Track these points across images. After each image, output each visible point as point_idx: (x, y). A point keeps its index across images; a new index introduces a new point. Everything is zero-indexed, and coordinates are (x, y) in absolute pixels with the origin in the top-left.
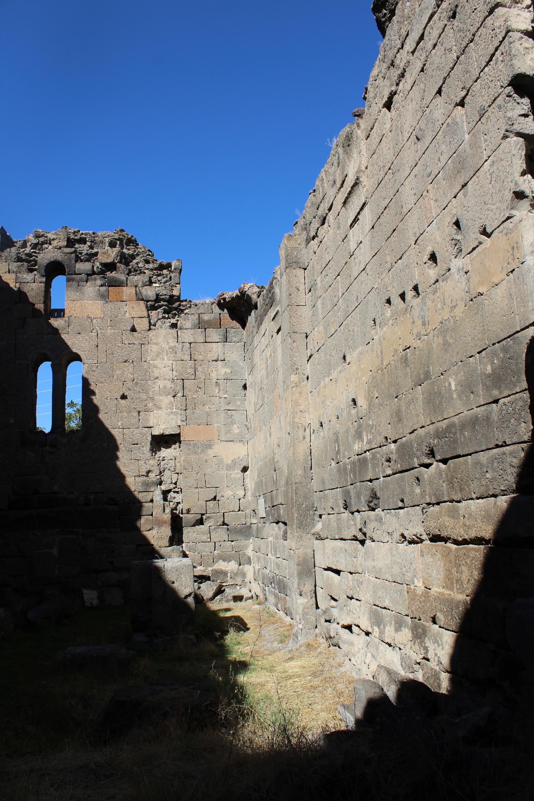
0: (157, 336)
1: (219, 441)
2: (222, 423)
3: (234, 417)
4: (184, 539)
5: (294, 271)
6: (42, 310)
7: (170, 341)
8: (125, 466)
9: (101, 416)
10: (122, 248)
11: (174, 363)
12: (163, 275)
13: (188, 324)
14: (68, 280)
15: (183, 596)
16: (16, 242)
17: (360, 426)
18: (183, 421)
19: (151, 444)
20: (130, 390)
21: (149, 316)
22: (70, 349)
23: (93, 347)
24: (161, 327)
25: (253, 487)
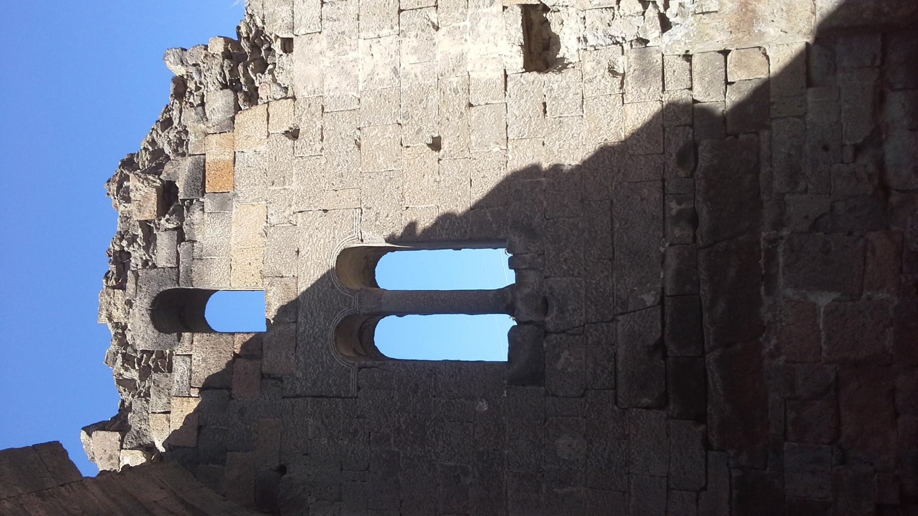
7: (317, 48)
8: (598, 128)
11: (362, 35)
13: (284, 12)
16: (123, 402)
22: (328, 272)
23: (326, 219)
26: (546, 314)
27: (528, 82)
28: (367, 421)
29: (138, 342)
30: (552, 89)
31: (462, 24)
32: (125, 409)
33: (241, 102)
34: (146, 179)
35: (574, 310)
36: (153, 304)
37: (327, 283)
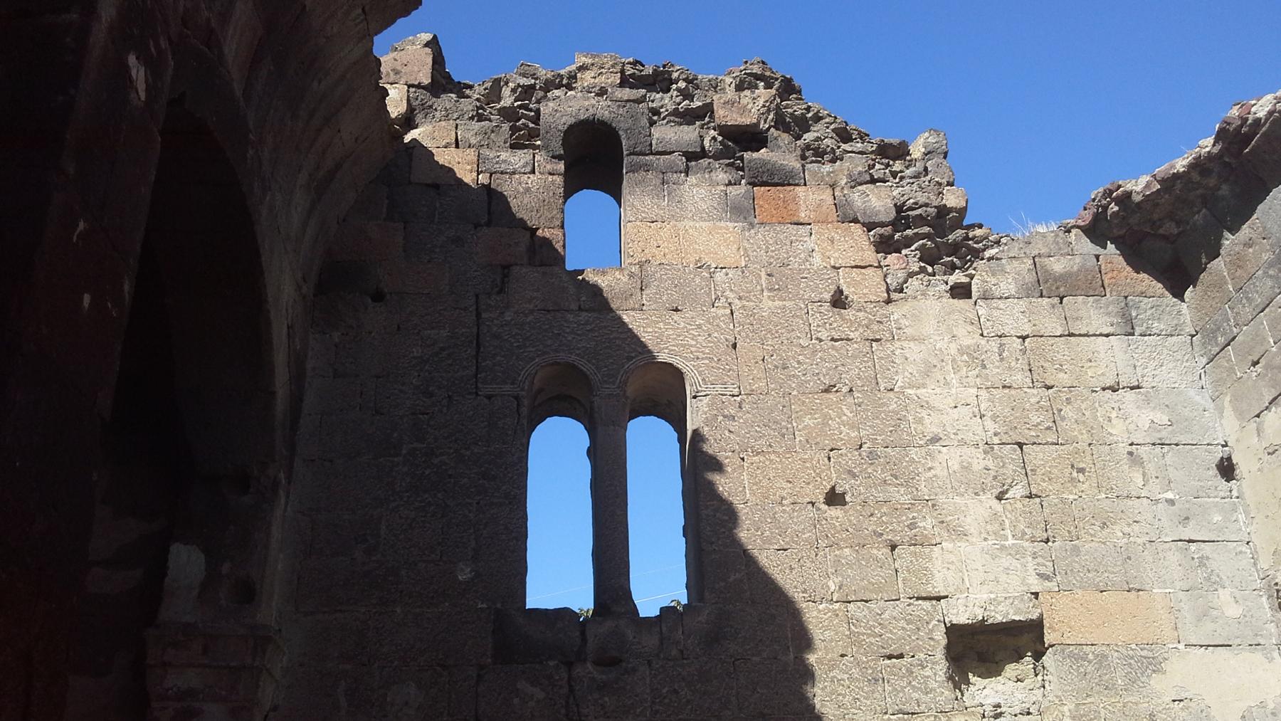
1: (1181, 646)
2: (1178, 585)
3: (1213, 565)
11: (983, 393)
13: (1007, 285)
16: (471, 87)
18: (1048, 578)
20: (854, 476)
22: (650, 352)
23: (723, 348)
26: (598, 663)
27: (931, 631)
28: (445, 410)
29: (551, 104)
30: (923, 667)
31: (1008, 533)
32: (461, 90)
33: (879, 230)
34: (769, 111)
35: (603, 706)
36: (602, 123)
37: (635, 350)
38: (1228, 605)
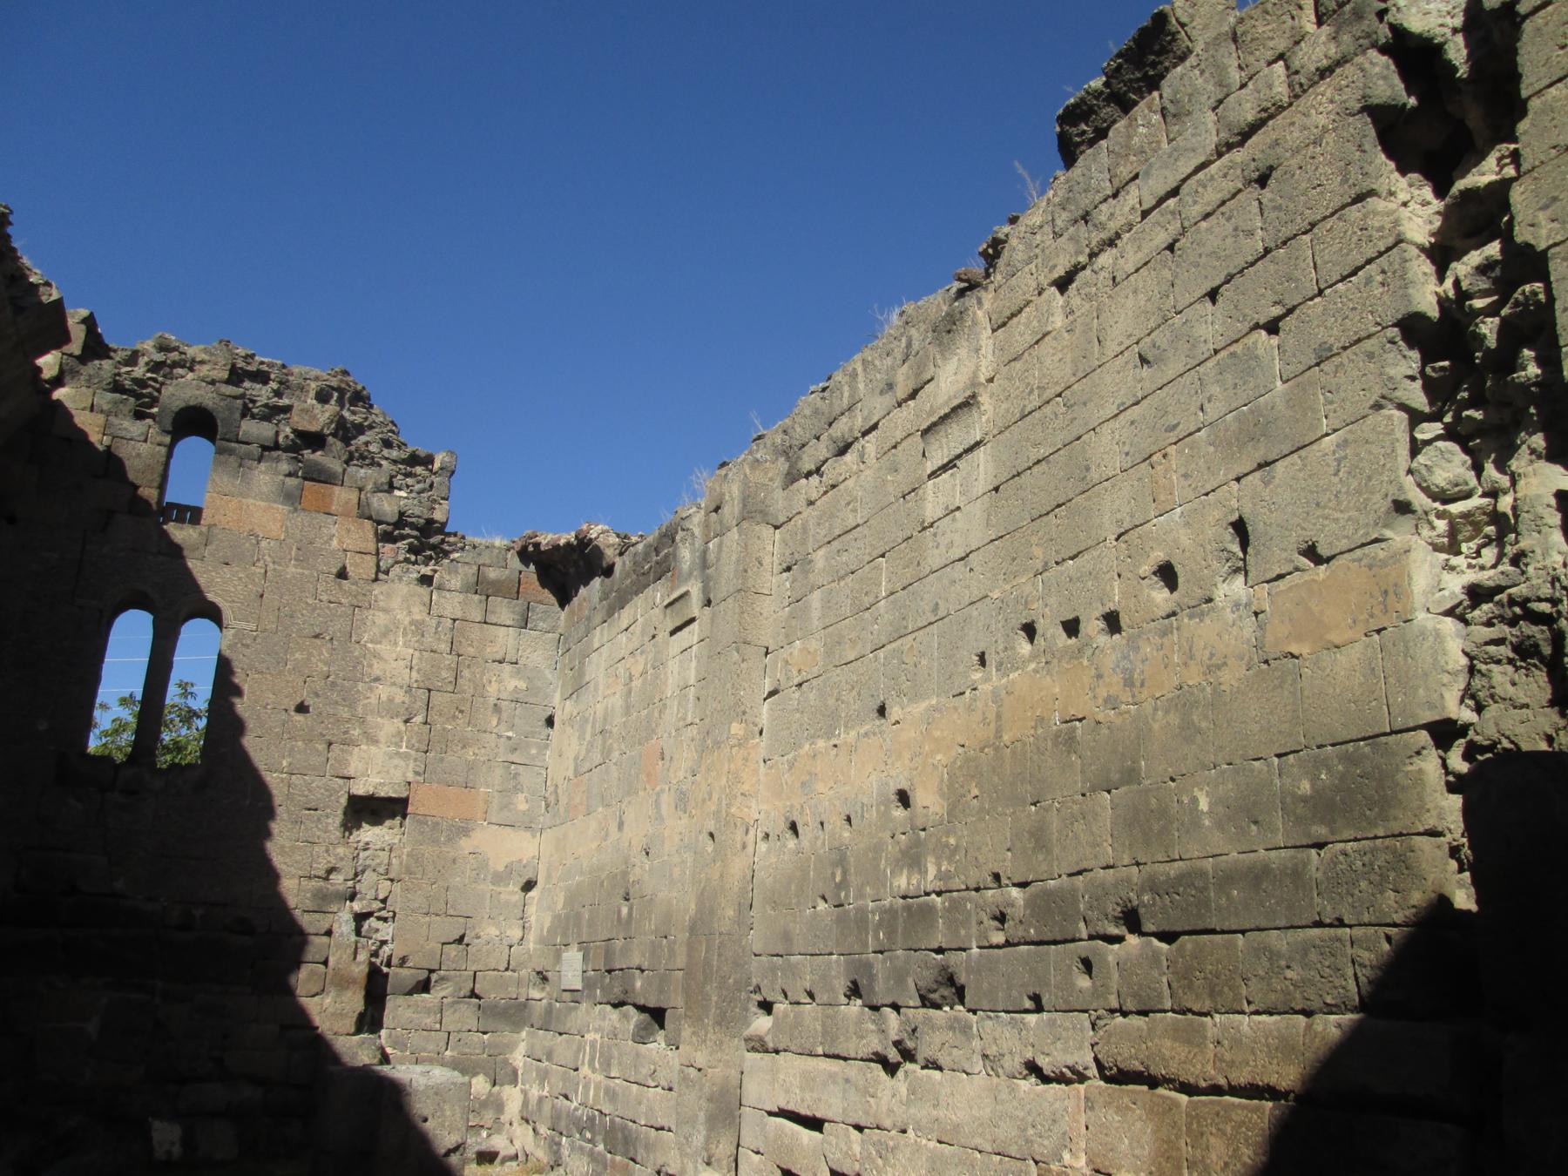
0: (389, 596)
3: (521, 779)
4: (388, 1019)
5: (757, 528)
6: (153, 502)
7: (415, 610)
9: (249, 742)
10: (342, 407)
11: (417, 654)
12: (416, 475)
13: (455, 582)
14: (220, 451)
15: (443, 1151)
17: (917, 843)
19: (345, 814)
20: (317, 695)
21: (377, 553)
24: (400, 579)
25: (547, 924)
38: (521, 803)
